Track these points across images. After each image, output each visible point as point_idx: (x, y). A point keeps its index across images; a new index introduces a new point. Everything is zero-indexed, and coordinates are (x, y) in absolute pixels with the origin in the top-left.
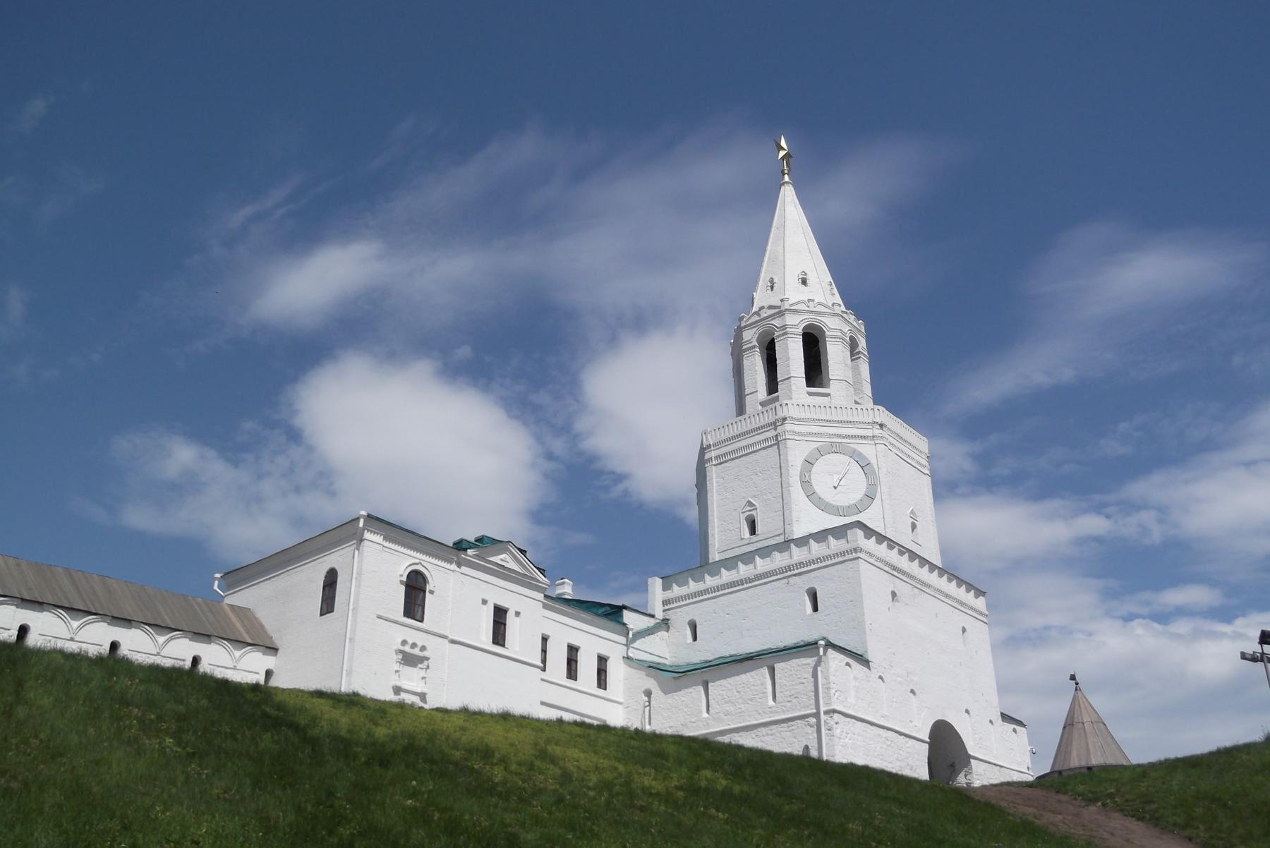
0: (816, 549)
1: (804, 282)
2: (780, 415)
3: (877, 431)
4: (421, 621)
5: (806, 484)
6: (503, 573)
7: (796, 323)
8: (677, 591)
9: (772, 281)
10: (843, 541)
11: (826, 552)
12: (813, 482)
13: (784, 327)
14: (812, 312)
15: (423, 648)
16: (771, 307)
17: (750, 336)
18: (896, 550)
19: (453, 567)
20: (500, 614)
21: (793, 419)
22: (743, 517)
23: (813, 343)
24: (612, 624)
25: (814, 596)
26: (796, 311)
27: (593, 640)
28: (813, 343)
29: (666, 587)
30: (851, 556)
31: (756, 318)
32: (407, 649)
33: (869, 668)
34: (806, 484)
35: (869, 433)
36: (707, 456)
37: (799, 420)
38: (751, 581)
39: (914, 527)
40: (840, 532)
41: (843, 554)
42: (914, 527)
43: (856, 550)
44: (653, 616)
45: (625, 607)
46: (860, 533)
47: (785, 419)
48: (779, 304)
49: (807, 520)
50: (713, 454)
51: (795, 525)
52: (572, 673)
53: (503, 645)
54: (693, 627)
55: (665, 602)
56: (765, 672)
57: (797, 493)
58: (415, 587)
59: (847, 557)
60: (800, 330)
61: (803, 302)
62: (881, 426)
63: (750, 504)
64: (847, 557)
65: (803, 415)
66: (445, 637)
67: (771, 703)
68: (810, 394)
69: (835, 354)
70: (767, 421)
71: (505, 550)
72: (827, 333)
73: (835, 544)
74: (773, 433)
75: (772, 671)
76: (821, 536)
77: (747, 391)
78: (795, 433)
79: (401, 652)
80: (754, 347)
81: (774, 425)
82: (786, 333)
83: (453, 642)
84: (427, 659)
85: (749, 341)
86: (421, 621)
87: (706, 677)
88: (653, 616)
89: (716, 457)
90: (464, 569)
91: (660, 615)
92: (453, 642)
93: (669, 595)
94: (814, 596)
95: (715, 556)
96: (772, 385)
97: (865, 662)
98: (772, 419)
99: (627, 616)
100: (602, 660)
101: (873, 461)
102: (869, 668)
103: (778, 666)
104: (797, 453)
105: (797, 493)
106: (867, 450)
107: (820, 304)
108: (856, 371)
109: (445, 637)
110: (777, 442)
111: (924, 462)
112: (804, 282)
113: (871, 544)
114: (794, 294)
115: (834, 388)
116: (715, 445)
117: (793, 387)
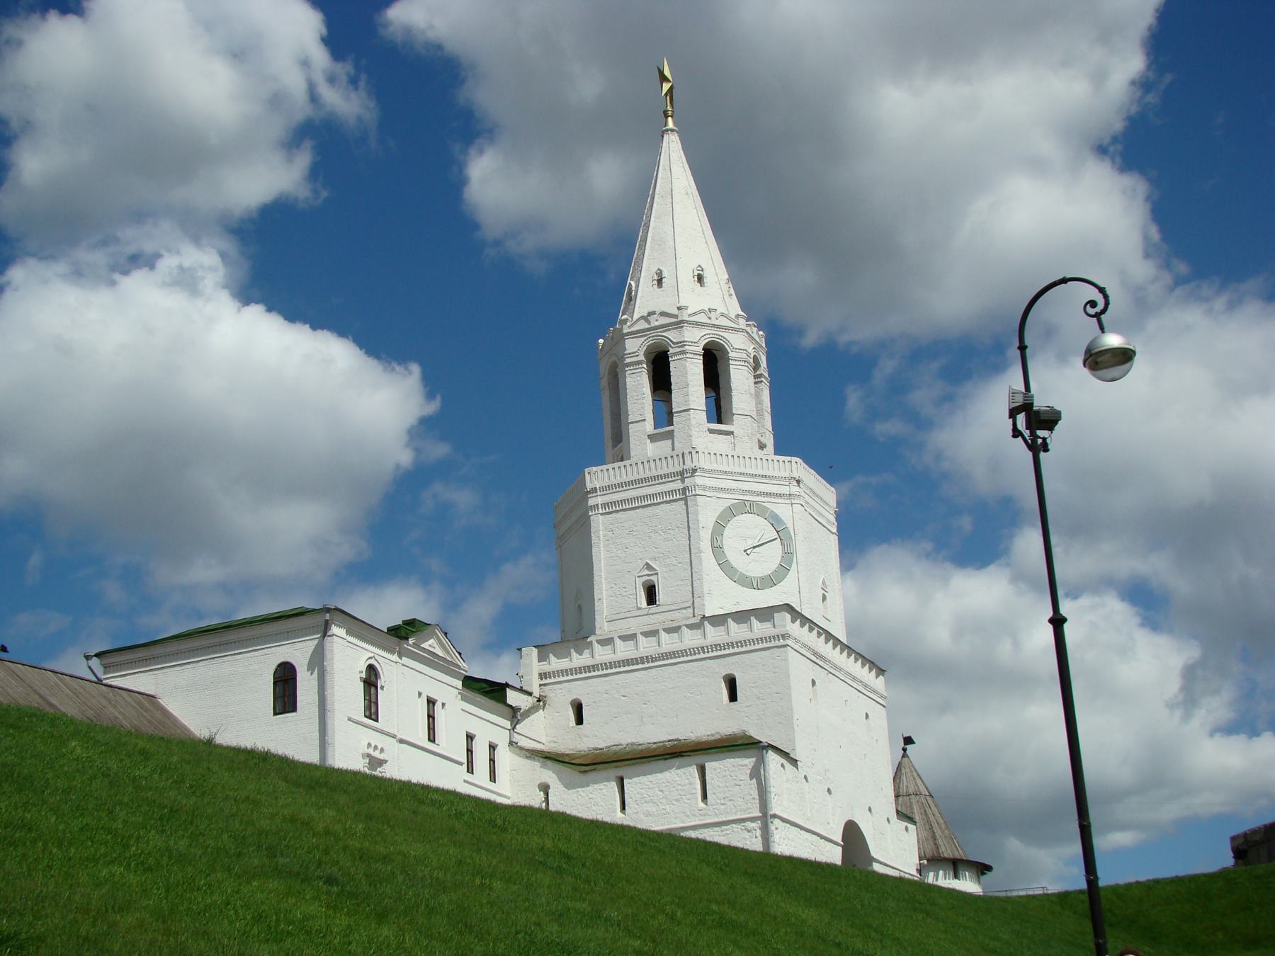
0: (736, 631)
1: (700, 279)
2: (689, 465)
3: (794, 489)
4: (377, 720)
5: (717, 549)
6: (432, 661)
7: (696, 339)
8: (555, 663)
9: (660, 273)
10: (768, 625)
11: (749, 636)
12: (726, 548)
13: (681, 344)
14: (714, 326)
15: (382, 750)
16: (663, 314)
17: (636, 348)
18: (815, 632)
19: (395, 657)
20: (431, 702)
21: (704, 470)
22: (640, 582)
23: (714, 361)
24: (492, 703)
25: (731, 684)
26: (697, 323)
27: (487, 726)
28: (714, 361)
29: (542, 658)
30: (777, 643)
31: (642, 325)
32: (371, 751)
33: (797, 767)
34: (717, 549)
35: (785, 490)
36: (591, 502)
37: (711, 471)
38: (653, 659)
39: (824, 598)
40: (765, 614)
41: (769, 639)
42: (824, 598)
43: (784, 636)
44: (530, 694)
45: (507, 685)
46: (788, 617)
47: (694, 471)
48: (676, 312)
49: (722, 596)
50: (600, 500)
51: (707, 597)
52: (470, 769)
53: (434, 741)
54: (578, 709)
55: (542, 676)
56: (693, 771)
57: (708, 562)
58: (371, 680)
59: (773, 644)
60: (700, 350)
61: (703, 311)
62: (798, 482)
63: (648, 566)
64: (773, 644)
65: (714, 467)
66: (394, 736)
67: (702, 805)
68: (711, 431)
69: (740, 379)
70: (671, 470)
71: (433, 635)
72: (731, 355)
73: (759, 628)
74: (678, 485)
75: (702, 771)
76: (742, 616)
77: (631, 419)
78: (705, 488)
79: (369, 755)
80: (640, 362)
81: (682, 475)
82: (684, 352)
83: (402, 741)
84: (385, 761)
85: (634, 354)
86: (377, 720)
87: (620, 772)
88: (530, 694)
89: (604, 505)
90: (405, 660)
91: (536, 693)
92: (402, 741)
93: (545, 667)
94: (731, 684)
95: (603, 627)
96: (665, 414)
97: (794, 762)
98: (678, 468)
99: (513, 698)
100: (492, 747)
101: (790, 525)
102: (797, 767)
103: (711, 766)
104: (707, 511)
105: (708, 562)
106: (782, 510)
107: (723, 315)
108: (758, 396)
109: (394, 736)
110: (685, 495)
111: (832, 519)
112: (700, 279)
113: (795, 628)
114: (694, 300)
115: (738, 425)
116: (602, 489)
117: (693, 422)
